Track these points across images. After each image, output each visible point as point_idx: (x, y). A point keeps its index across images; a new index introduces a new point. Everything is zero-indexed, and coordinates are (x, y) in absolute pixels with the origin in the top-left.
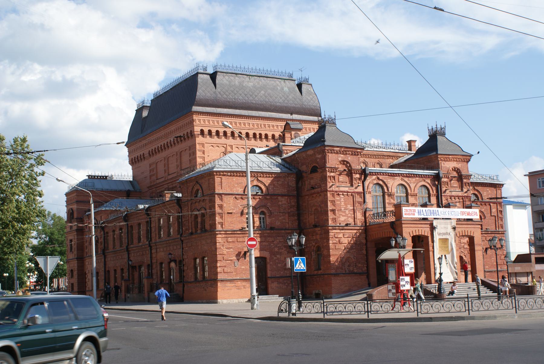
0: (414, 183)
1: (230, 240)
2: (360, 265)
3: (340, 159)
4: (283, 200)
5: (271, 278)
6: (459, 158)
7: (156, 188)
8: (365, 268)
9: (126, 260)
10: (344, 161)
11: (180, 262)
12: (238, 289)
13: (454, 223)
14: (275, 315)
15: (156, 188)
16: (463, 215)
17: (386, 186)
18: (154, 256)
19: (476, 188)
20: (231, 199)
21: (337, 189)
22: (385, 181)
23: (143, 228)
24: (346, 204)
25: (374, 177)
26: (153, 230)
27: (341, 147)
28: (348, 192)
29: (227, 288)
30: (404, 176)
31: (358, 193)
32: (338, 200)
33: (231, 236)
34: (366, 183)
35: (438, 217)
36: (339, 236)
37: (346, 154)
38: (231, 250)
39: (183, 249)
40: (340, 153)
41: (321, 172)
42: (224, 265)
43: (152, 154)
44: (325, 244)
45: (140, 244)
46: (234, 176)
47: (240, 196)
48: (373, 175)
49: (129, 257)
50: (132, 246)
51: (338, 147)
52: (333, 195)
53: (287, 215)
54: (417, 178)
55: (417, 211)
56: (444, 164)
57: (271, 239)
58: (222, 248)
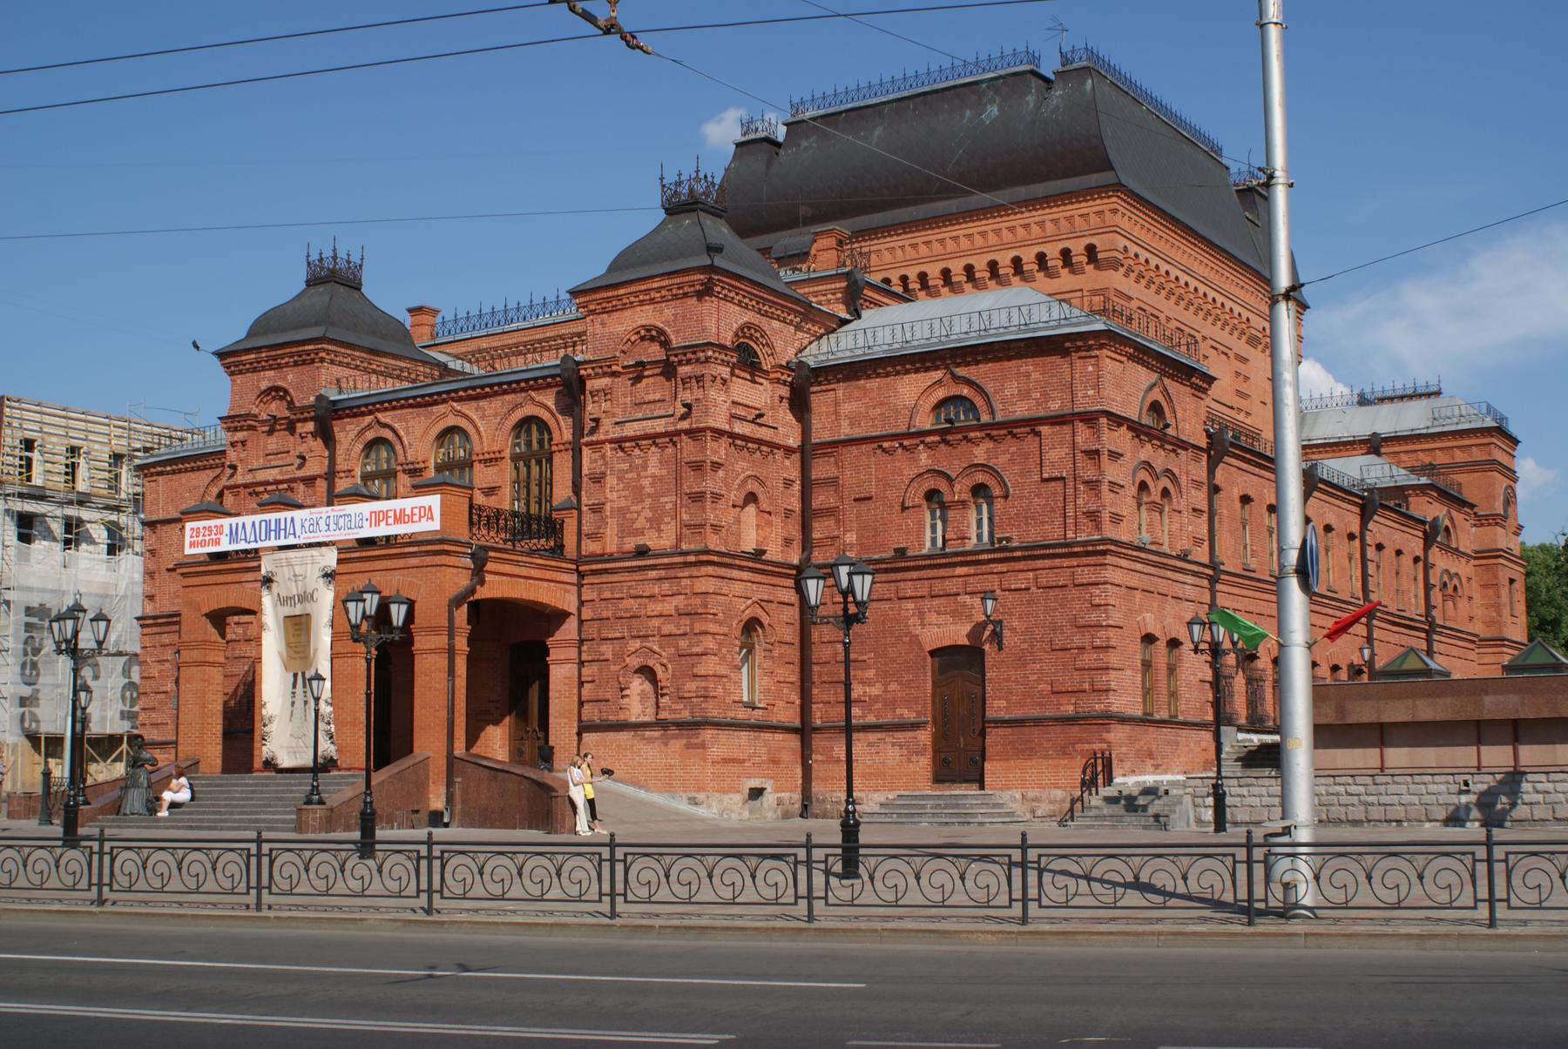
0: (495, 415)
3: (264, 385)
6: (659, 289)
13: (330, 558)
16: (378, 523)
19: (961, 371)
21: (249, 479)
27: (258, 349)
30: (460, 400)
35: (291, 541)
37: (280, 367)
40: (264, 369)
42: (151, 705)
46: (180, 471)
48: (363, 414)
54: (508, 397)
55: (226, 530)
56: (603, 324)
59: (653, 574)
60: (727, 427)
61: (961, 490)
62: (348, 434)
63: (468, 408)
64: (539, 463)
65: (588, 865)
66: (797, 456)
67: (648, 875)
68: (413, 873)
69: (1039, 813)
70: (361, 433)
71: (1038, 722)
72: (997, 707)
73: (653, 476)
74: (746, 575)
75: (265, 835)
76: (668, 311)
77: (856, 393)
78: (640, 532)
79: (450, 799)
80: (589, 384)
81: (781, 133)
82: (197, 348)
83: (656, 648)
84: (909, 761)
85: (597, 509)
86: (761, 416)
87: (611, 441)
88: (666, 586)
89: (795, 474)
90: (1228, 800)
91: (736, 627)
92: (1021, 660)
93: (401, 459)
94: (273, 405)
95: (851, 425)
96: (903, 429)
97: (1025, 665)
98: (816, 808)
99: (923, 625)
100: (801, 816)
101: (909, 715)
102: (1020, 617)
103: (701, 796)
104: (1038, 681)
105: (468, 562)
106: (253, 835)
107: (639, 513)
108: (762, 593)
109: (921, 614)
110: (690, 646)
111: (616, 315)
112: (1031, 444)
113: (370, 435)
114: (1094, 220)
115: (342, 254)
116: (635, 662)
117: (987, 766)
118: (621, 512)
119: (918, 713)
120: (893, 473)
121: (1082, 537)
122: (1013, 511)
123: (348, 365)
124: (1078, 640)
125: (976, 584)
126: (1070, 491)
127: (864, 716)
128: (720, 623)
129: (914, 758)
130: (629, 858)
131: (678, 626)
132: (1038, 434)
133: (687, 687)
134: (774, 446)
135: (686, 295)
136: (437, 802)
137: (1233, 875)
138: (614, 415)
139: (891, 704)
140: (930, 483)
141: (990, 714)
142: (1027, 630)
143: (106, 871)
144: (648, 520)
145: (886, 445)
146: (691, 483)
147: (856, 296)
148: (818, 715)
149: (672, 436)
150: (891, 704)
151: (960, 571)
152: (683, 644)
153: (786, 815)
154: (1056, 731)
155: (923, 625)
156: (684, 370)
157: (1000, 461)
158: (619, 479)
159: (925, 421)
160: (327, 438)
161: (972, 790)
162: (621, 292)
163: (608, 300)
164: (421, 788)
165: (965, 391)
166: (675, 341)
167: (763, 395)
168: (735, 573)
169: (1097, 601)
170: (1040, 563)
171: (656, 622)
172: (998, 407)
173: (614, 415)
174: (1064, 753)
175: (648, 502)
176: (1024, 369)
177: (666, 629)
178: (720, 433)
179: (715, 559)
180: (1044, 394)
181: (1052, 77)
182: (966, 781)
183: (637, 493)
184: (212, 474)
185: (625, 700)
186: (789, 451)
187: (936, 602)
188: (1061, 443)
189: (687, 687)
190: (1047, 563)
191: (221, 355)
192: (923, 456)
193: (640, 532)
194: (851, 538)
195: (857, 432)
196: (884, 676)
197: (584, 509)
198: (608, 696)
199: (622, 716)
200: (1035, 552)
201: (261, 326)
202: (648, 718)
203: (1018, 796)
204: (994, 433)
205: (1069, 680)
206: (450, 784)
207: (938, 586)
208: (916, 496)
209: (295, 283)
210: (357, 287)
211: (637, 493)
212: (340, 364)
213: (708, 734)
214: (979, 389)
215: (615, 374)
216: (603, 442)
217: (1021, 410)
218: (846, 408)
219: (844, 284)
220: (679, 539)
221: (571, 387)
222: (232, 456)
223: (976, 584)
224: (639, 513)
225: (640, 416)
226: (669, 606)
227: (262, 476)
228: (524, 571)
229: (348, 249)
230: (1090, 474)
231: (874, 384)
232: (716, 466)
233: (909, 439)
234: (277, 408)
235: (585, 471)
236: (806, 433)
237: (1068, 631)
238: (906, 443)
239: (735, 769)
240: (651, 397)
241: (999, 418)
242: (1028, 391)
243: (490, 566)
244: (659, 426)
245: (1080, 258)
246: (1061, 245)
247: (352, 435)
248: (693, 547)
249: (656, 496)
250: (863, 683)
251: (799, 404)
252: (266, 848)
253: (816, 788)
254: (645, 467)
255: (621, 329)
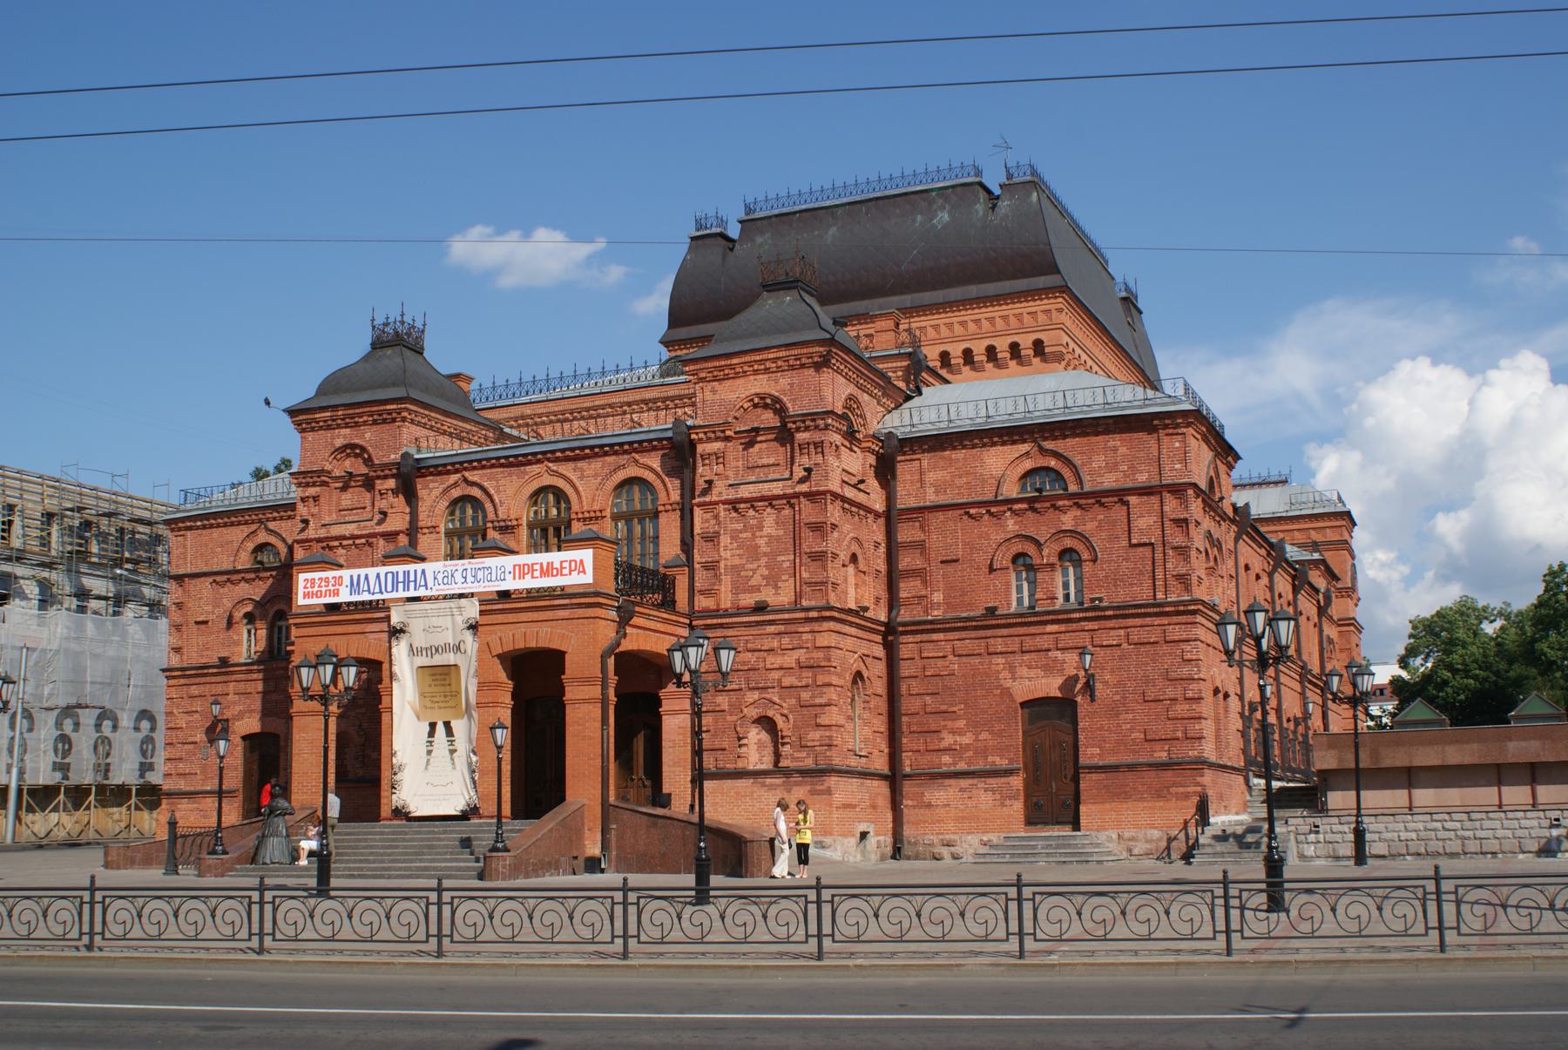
0: (595, 476)
3: (339, 442)
6: (774, 360)
13: (472, 610)
16: (522, 576)
19: (1048, 445)
20: (204, 587)
21: (322, 533)
25: (454, 478)
27: (334, 408)
30: (557, 460)
33: (197, 680)
35: (422, 592)
37: (357, 425)
38: (196, 716)
40: (339, 426)
46: (211, 526)
47: (225, 577)
48: (448, 473)
54: (608, 459)
55: (347, 581)
56: (714, 391)
59: (772, 629)
60: (839, 491)
61: (1049, 553)
62: (432, 494)
63: (566, 469)
64: (641, 521)
65: (601, 909)
66: (882, 521)
67: (1057, 914)
68: (422, 918)
69: (1136, 851)
70: (446, 491)
71: (1132, 767)
72: (1090, 754)
73: (769, 536)
74: (853, 631)
75: (446, 883)
76: (784, 381)
77: (941, 463)
78: (757, 589)
79: (605, 846)
80: (700, 448)
81: (734, 231)
82: (267, 403)
83: (776, 699)
84: (1003, 805)
85: (711, 567)
86: (862, 482)
87: (725, 502)
88: (786, 640)
89: (880, 537)
90: (1368, 836)
91: (849, 677)
92: (1114, 711)
93: (491, 516)
94: (347, 463)
95: (937, 492)
96: (990, 497)
97: (1117, 715)
98: (907, 850)
99: (1014, 679)
100: (893, 857)
101: (1001, 762)
102: (1112, 671)
103: (828, 840)
104: (1131, 730)
105: (613, 614)
106: (434, 883)
107: (754, 571)
108: (864, 648)
109: (1012, 669)
110: (813, 697)
111: (727, 383)
112: (1119, 512)
113: (456, 493)
114: (1042, 318)
115: (408, 319)
116: (753, 713)
117: (1083, 808)
118: (736, 570)
119: (1011, 761)
120: (980, 537)
121: (1172, 598)
122: (1102, 574)
123: (424, 426)
124: (1170, 692)
125: (1066, 640)
126: (1159, 556)
127: (955, 764)
128: (839, 675)
129: (1008, 802)
130: (1038, 898)
131: (800, 678)
132: (1127, 504)
133: (810, 736)
134: (869, 510)
135: (803, 366)
136: (595, 850)
137: (1006, 913)
138: (727, 478)
139: (984, 752)
140: (1019, 547)
141: (1083, 761)
142: (1119, 683)
143: (86, 917)
144: (764, 577)
145: (972, 511)
146: (810, 542)
147: (918, 373)
148: (908, 762)
149: (790, 499)
150: (984, 752)
151: (1050, 628)
152: (805, 695)
153: (883, 858)
154: (1151, 777)
155: (1014, 679)
156: (801, 437)
157: (1088, 527)
158: (732, 538)
159: (1011, 490)
160: (410, 494)
161: (1066, 831)
162: (735, 361)
163: (721, 369)
164: (573, 832)
165: (1053, 463)
166: (792, 410)
167: (857, 462)
168: (846, 629)
169: (1188, 656)
170: (1130, 622)
171: (776, 675)
172: (1086, 478)
173: (727, 478)
174: (1159, 796)
175: (764, 561)
176: (1111, 444)
177: (787, 681)
178: (836, 496)
179: (836, 614)
180: (1132, 467)
181: (997, 191)
182: (1058, 823)
183: (753, 552)
184: (246, 530)
185: (744, 749)
186: (877, 515)
187: (1027, 657)
188: (1149, 513)
189: (810, 736)
190: (1138, 621)
191: (292, 412)
192: (1010, 522)
193: (757, 589)
194: (938, 597)
195: (943, 499)
196: (975, 726)
197: (697, 566)
198: (725, 745)
199: (740, 764)
200: (1124, 612)
201: (330, 385)
202: (767, 765)
203: (1115, 836)
204: (1082, 502)
205: (1163, 729)
206: (605, 831)
207: (1029, 643)
208: (1002, 559)
209: (362, 345)
210: (420, 352)
211: (753, 552)
212: (419, 424)
213: (832, 781)
214: (1068, 462)
215: (728, 439)
216: (717, 503)
217: (1109, 481)
218: (931, 477)
219: (905, 363)
220: (798, 596)
221: (680, 453)
222: (302, 510)
223: (1066, 640)
224: (754, 571)
225: (753, 479)
226: (790, 659)
227: (336, 531)
228: (652, 625)
229: (414, 315)
230: (1178, 539)
231: (960, 454)
232: (834, 526)
233: (996, 506)
234: (349, 465)
235: (697, 530)
236: (890, 499)
237: (1160, 683)
238: (993, 510)
239: (850, 813)
240: (765, 461)
241: (1087, 488)
242: (1116, 464)
243: (635, 620)
244: (777, 489)
245: (1027, 352)
246: (1010, 340)
247: (436, 492)
248: (813, 603)
249: (772, 555)
250: (953, 732)
251: (885, 470)
252: (268, 896)
253: (908, 832)
254: (761, 528)
255: (733, 396)
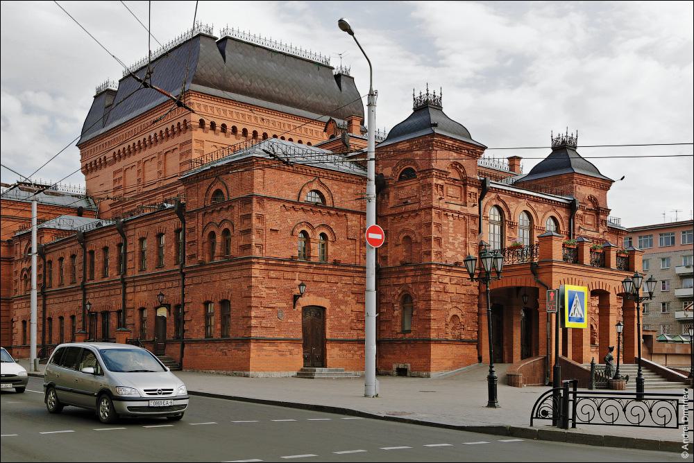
0: (542, 211)
1: (272, 274)
2: (469, 328)
4: (354, 219)
5: (331, 341)
7: (122, 206)
8: (476, 334)
9: (80, 303)
10: (457, 164)
11: (178, 307)
12: (282, 355)
14: (523, 423)
15: (122, 206)
17: (509, 211)
18: (129, 297)
20: (277, 207)
21: (445, 206)
22: (507, 203)
23: (113, 255)
24: (455, 232)
25: (493, 195)
26: (130, 257)
27: (455, 140)
28: (459, 213)
29: (264, 353)
31: (473, 217)
32: (445, 225)
33: (275, 268)
34: (483, 203)
36: (444, 281)
38: (274, 291)
39: (184, 286)
40: (453, 150)
41: (422, 178)
42: (262, 315)
43: (118, 157)
44: (422, 292)
45: (106, 280)
47: (291, 205)
49: (85, 299)
50: (91, 282)
51: (451, 139)
52: (439, 214)
53: (358, 243)
54: (546, 205)
57: (333, 279)
58: (260, 286)
111: (583, 187)
162: (588, 179)
